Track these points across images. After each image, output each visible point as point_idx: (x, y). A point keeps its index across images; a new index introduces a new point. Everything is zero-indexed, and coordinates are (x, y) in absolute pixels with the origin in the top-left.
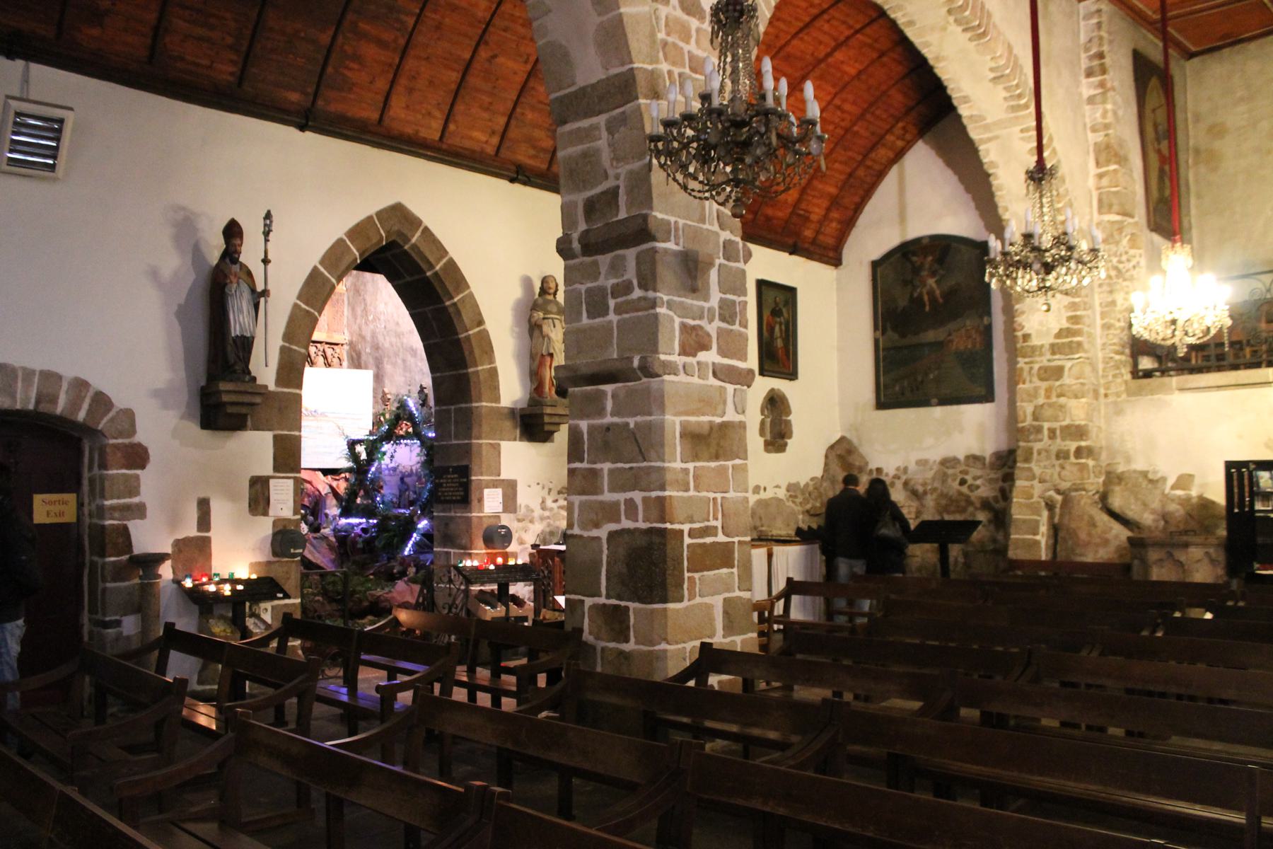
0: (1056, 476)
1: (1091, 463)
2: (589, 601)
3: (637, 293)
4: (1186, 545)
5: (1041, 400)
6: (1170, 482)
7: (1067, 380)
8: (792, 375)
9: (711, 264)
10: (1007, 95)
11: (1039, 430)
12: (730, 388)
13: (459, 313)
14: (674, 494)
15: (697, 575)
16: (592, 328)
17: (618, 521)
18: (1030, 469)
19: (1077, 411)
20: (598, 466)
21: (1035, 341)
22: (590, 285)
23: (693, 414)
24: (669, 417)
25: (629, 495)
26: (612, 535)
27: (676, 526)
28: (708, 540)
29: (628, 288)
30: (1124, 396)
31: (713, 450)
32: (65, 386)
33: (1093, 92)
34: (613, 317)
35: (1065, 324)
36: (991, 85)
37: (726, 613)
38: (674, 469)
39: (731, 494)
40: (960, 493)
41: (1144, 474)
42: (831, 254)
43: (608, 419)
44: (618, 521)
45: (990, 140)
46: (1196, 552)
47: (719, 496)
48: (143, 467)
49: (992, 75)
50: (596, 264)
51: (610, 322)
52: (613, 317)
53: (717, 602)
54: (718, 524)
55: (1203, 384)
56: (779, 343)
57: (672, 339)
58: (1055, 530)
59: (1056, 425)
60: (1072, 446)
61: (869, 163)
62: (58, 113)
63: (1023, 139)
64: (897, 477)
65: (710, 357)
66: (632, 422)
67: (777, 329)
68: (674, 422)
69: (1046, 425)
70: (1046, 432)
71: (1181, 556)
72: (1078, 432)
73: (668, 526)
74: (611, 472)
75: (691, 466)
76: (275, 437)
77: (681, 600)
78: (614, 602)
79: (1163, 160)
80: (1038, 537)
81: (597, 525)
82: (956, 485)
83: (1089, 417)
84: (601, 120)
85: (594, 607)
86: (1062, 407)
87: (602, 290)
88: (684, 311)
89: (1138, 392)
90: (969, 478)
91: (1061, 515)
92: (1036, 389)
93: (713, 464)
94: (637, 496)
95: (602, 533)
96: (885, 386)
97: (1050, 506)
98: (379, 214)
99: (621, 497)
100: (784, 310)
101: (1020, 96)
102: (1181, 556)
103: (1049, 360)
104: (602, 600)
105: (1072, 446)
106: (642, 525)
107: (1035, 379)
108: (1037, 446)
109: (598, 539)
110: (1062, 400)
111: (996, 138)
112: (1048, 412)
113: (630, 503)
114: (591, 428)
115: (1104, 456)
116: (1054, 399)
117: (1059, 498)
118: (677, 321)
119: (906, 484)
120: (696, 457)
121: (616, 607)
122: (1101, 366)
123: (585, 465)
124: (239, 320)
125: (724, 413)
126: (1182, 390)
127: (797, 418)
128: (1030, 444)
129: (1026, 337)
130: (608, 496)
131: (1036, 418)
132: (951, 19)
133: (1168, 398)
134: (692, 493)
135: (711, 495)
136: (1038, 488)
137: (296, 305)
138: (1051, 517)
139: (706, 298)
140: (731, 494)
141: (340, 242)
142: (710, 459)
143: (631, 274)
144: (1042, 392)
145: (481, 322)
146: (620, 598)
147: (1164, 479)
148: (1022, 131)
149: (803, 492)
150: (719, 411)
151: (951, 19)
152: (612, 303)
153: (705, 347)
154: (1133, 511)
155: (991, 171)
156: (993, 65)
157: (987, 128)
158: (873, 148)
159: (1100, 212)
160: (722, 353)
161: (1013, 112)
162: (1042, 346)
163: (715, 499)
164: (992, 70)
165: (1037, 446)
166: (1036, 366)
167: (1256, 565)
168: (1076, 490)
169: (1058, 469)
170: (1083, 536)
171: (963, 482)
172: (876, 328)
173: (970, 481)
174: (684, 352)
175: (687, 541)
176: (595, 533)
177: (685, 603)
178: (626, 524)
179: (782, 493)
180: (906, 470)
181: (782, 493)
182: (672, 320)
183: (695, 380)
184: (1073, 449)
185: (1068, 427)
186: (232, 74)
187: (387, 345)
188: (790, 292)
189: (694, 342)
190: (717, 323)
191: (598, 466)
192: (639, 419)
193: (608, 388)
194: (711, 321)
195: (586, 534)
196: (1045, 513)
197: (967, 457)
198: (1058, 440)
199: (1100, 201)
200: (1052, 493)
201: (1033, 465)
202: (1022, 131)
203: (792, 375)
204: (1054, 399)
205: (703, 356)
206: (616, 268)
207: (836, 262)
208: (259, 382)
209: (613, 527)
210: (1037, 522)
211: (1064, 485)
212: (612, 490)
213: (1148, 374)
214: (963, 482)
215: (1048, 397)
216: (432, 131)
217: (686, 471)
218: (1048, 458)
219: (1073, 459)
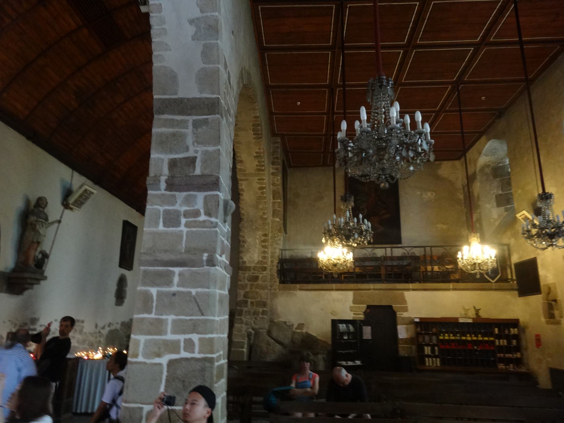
0: (252, 322)
3: (203, 218)
5: (248, 289)
6: (295, 326)
7: (260, 282)
10: (258, 164)
11: (246, 302)
16: (166, 233)
18: (241, 319)
20: (164, 317)
22: (167, 208)
25: (188, 336)
29: (197, 213)
30: (278, 290)
33: (274, 171)
34: (183, 228)
35: (261, 259)
36: (254, 158)
41: (285, 323)
44: (178, 352)
45: (244, 180)
49: (255, 155)
50: (174, 196)
51: (182, 231)
52: (183, 228)
55: (309, 288)
59: (254, 300)
63: (258, 183)
66: (194, 291)
69: (249, 300)
70: (249, 303)
74: (174, 321)
84: (191, 119)
86: (257, 293)
94: (195, 337)
95: (164, 360)
99: (181, 337)
103: (252, 273)
105: (261, 310)
106: (197, 355)
108: (245, 309)
109: (160, 364)
114: (159, 294)
117: (253, 332)
123: (153, 316)
126: (300, 290)
128: (242, 308)
129: (244, 262)
130: (170, 337)
131: (245, 296)
133: (295, 292)
136: (244, 327)
144: (249, 286)
147: (293, 325)
148: (259, 179)
152: (183, 221)
154: (281, 338)
155: (241, 193)
156: (258, 151)
157: (245, 175)
161: (258, 171)
162: (250, 267)
164: (256, 153)
165: (245, 309)
168: (261, 329)
169: (254, 319)
176: (157, 360)
178: (184, 354)
179: (118, 327)
181: (118, 327)
191: (164, 317)
192: (200, 290)
193: (177, 270)
195: (148, 361)
198: (255, 307)
200: (251, 330)
202: (259, 179)
204: (254, 289)
211: (256, 327)
212: (174, 332)
215: (251, 288)
218: (249, 314)
219: (261, 316)
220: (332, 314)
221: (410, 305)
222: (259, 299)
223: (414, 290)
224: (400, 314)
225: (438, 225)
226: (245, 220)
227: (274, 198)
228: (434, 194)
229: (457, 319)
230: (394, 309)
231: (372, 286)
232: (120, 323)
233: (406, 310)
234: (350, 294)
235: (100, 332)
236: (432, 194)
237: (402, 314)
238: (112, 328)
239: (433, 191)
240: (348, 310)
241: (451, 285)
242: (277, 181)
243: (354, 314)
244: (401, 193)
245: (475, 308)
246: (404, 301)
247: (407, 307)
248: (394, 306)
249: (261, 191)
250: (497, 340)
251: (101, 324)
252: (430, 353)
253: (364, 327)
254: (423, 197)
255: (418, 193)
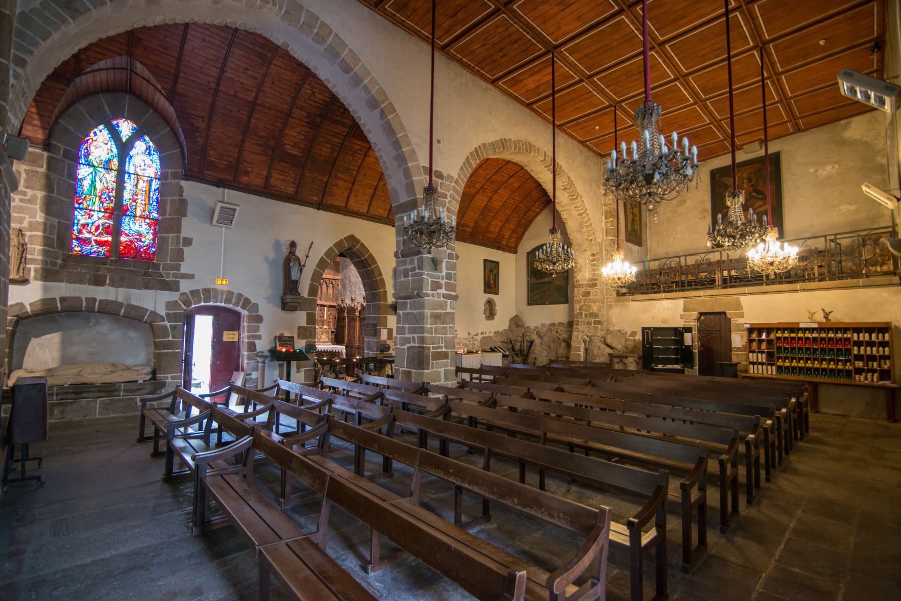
0: (587, 331)
1: (599, 326)
2: (401, 369)
3: (417, 271)
4: (626, 357)
5: (582, 304)
6: (628, 334)
7: (591, 297)
8: (497, 293)
9: (442, 261)
10: (568, 195)
11: (581, 314)
12: (449, 301)
13: (373, 272)
14: (427, 335)
15: (435, 362)
16: (404, 281)
17: (410, 343)
18: (578, 328)
19: (595, 308)
21: (581, 283)
23: (435, 310)
24: (426, 311)
25: (413, 335)
26: (408, 348)
27: (428, 346)
28: (439, 350)
29: (414, 269)
31: (442, 321)
32: (235, 296)
34: (410, 278)
35: (591, 276)
37: (445, 374)
38: (427, 328)
39: (448, 336)
40: (556, 336)
41: (619, 331)
42: (513, 250)
43: (408, 311)
44: (410, 343)
45: (564, 210)
46: (631, 360)
47: (444, 336)
48: (261, 323)
50: (406, 260)
52: (410, 278)
53: (442, 370)
54: (443, 345)
56: (492, 282)
57: (428, 286)
58: (586, 350)
59: (587, 312)
60: (593, 320)
61: (526, 217)
62: (234, 207)
63: (575, 210)
64: (534, 330)
65: (442, 291)
66: (415, 312)
67: (491, 277)
68: (428, 312)
69: (584, 313)
71: (625, 360)
72: (596, 316)
73: (425, 345)
74: (408, 327)
75: (433, 326)
76: (307, 313)
77: (429, 369)
78: (408, 369)
79: (634, 215)
80: (580, 353)
81: (404, 345)
82: (554, 333)
83: (599, 310)
85: (402, 371)
86: (589, 306)
87: (407, 269)
88: (432, 276)
89: (618, 301)
90: (559, 331)
91: (589, 345)
92: (581, 299)
93: (442, 326)
94: (416, 336)
95: (405, 347)
96: (531, 298)
97: (585, 342)
98: (345, 238)
99: (411, 336)
100: (494, 270)
101: (573, 195)
102: (625, 360)
104: (405, 369)
105: (593, 320)
107: (580, 296)
108: (581, 320)
109: (404, 349)
110: (590, 303)
111: (566, 210)
112: (584, 308)
113: (413, 338)
114: (403, 313)
115: (605, 324)
116: (587, 303)
117: (588, 339)
118: (430, 280)
119: (537, 332)
120: (436, 323)
121: (409, 371)
122: (605, 292)
123: (401, 325)
124: (294, 275)
125: (446, 309)
127: (498, 308)
129: (578, 281)
130: (407, 335)
131: (580, 309)
132: (546, 169)
134: (434, 335)
135: (441, 336)
136: (580, 335)
137: (315, 269)
138: (585, 345)
139: (441, 272)
140: (448, 336)
141: (331, 248)
142: (441, 324)
143: (416, 265)
145: (381, 275)
146: (410, 368)
147: (626, 333)
149: (500, 334)
150: (445, 309)
151: (546, 169)
152: (410, 273)
153: (441, 288)
154: (615, 344)
156: (563, 184)
157: (563, 206)
158: (527, 212)
159: (606, 236)
160: (446, 289)
163: (442, 337)
164: (562, 186)
165: (581, 320)
166: (581, 291)
167: (653, 365)
170: (595, 352)
171: (557, 332)
172: (528, 276)
173: (560, 332)
174: (432, 290)
175: (432, 350)
176: (403, 347)
177: (430, 370)
178: (412, 344)
179: (492, 335)
180: (537, 327)
182: (428, 280)
183: (436, 299)
184: (593, 321)
185: (591, 313)
186: (293, 191)
187: (353, 281)
188: (497, 264)
189: (436, 286)
190: (445, 280)
192: (417, 311)
193: (409, 301)
194: (442, 279)
196: (583, 344)
197: (558, 323)
198: (588, 318)
199: (606, 232)
201: (579, 327)
203: (497, 293)
204: (587, 303)
205: (439, 291)
206: (412, 262)
207: (516, 252)
208: (301, 295)
209: (409, 345)
210: (580, 347)
211: (589, 334)
212: (409, 334)
213: (624, 295)
214: (557, 332)
216: (364, 209)
217: (432, 328)
218: (584, 324)
219: (593, 325)
220: (662, 322)
221: (745, 310)
222: (591, 311)
223: (751, 294)
224: (734, 321)
225: (841, 207)
226: (575, 244)
227: (606, 218)
228: (836, 166)
229: (798, 324)
230: (728, 315)
231: (702, 293)
232: (493, 332)
233: (742, 316)
234: (681, 303)
235: (473, 338)
236: (833, 168)
237: (737, 321)
238: (485, 335)
239: (836, 163)
240: (679, 317)
241: (798, 286)
242: (608, 201)
243: (685, 322)
244: (785, 175)
245: (824, 310)
246: (739, 306)
247: (743, 312)
248: (727, 312)
249: (580, 217)
250: (856, 348)
251: (473, 333)
252: (764, 361)
253: (685, 334)
254: (818, 174)
255: (812, 170)
